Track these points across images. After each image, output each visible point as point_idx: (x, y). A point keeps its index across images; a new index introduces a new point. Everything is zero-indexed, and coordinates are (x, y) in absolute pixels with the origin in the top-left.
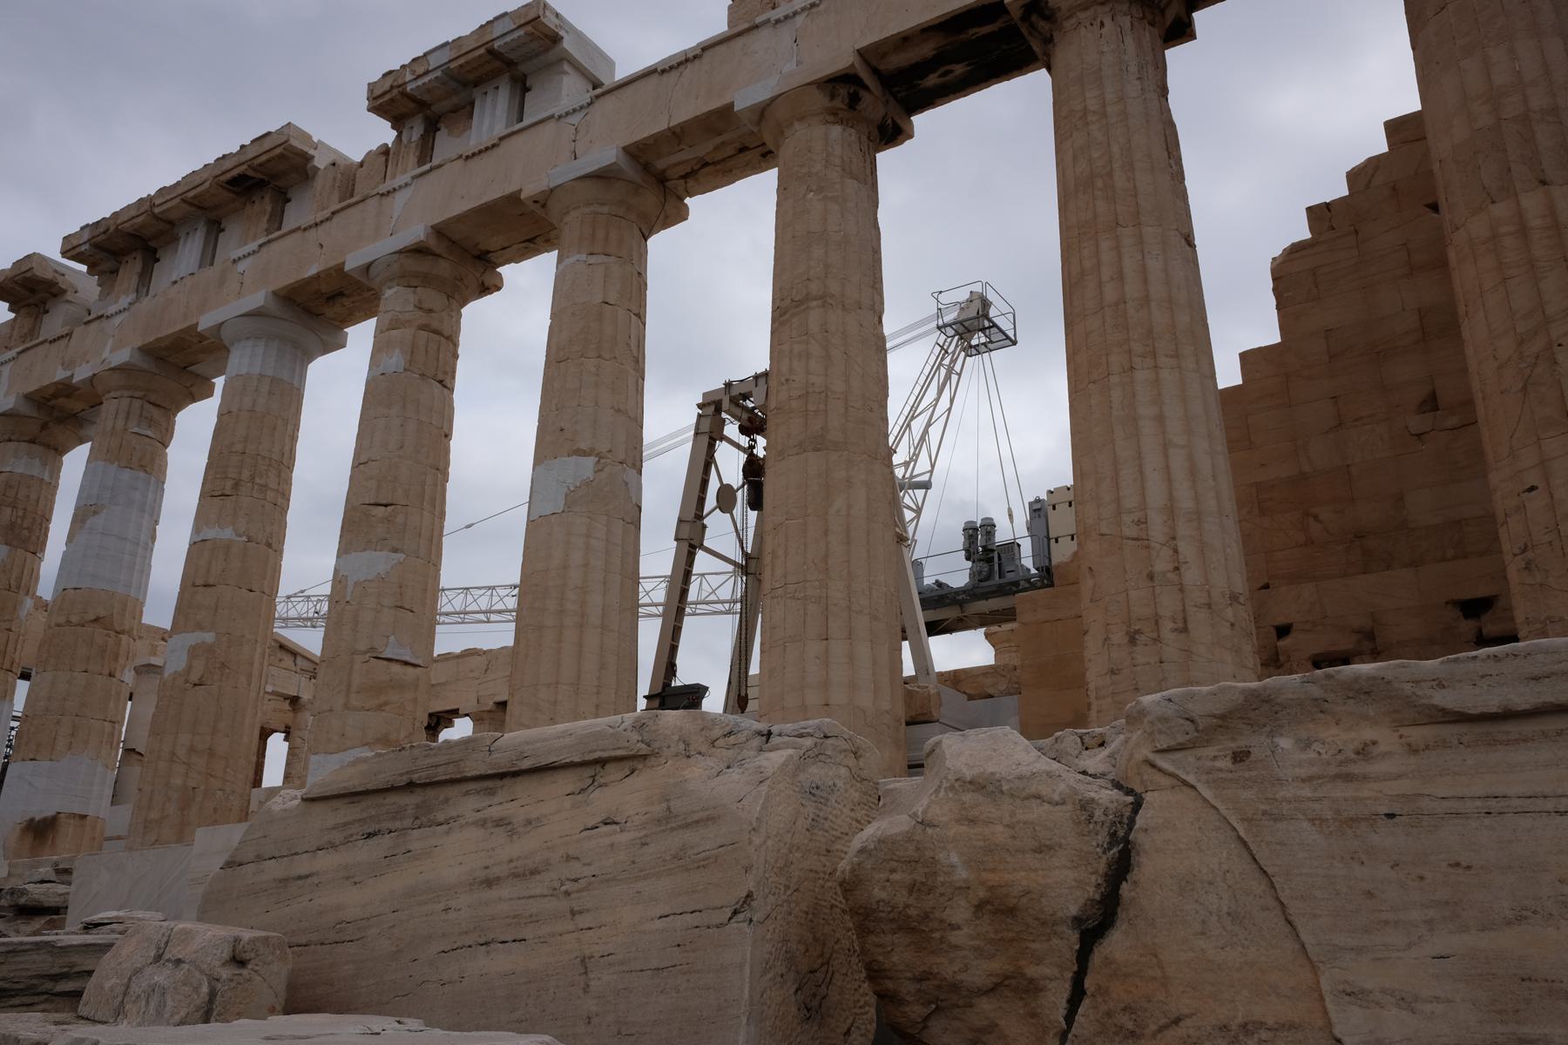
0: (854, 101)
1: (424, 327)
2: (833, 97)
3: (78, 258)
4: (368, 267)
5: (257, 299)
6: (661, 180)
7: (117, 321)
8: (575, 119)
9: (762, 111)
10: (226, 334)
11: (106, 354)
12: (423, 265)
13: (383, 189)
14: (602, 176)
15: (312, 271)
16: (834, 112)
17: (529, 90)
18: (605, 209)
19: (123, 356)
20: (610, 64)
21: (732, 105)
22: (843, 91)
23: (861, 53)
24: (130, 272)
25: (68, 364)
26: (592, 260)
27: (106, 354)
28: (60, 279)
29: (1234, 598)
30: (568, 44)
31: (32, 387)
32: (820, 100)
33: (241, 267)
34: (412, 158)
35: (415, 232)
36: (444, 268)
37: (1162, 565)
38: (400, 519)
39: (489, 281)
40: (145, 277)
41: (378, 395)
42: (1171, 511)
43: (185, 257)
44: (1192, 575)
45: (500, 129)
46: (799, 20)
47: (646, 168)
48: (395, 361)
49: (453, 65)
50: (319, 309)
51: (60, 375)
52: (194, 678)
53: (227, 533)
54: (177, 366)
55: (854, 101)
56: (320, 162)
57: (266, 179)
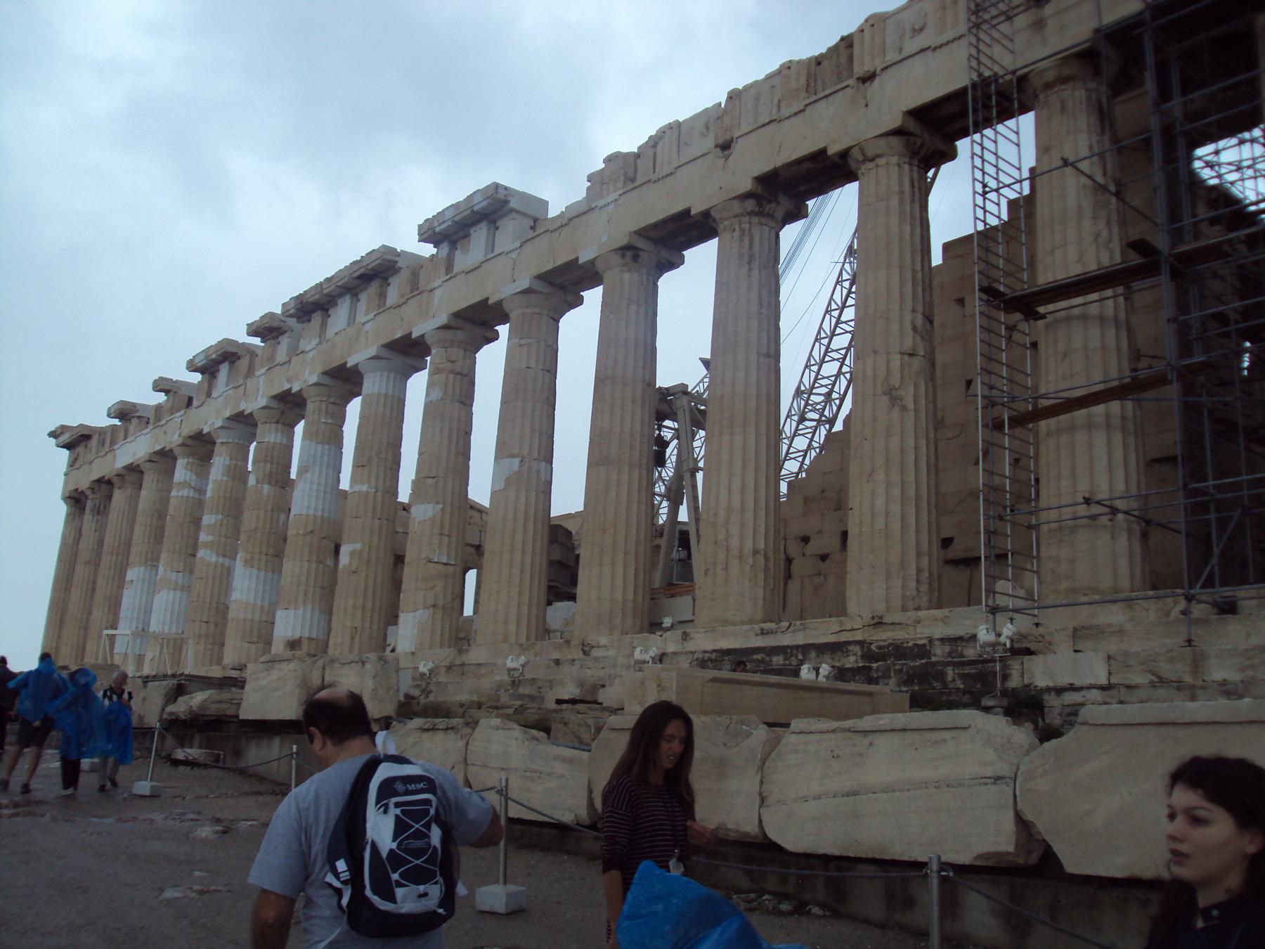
0: (636, 258)
1: (451, 372)
2: (623, 256)
3: (291, 316)
4: (423, 336)
5: (373, 351)
6: (562, 287)
7: (311, 354)
8: (514, 255)
9: (592, 262)
10: (361, 369)
11: (306, 377)
12: (449, 335)
13: (429, 287)
14: (527, 292)
15: (398, 336)
16: (625, 265)
17: (497, 228)
18: (528, 310)
19: (314, 379)
20: (544, 204)
21: (577, 259)
22: (629, 254)
23: (631, 234)
24: (317, 318)
25: (289, 381)
26: (522, 342)
27: (306, 377)
28: (283, 325)
29: (756, 552)
30: (513, 204)
31: (275, 393)
32: (617, 259)
33: (367, 327)
34: (443, 270)
35: (442, 319)
36: (460, 335)
37: (721, 537)
38: (441, 485)
39: (489, 335)
40: (324, 326)
41: (431, 412)
42: (729, 510)
43: (340, 315)
44: (734, 543)
45: (481, 257)
46: (611, 207)
47: (551, 283)
48: (437, 394)
49: (456, 219)
50: (408, 351)
51: (287, 387)
52: (353, 568)
53: (365, 488)
54: (345, 380)
55: (636, 258)
56: (401, 263)
57: (376, 273)
